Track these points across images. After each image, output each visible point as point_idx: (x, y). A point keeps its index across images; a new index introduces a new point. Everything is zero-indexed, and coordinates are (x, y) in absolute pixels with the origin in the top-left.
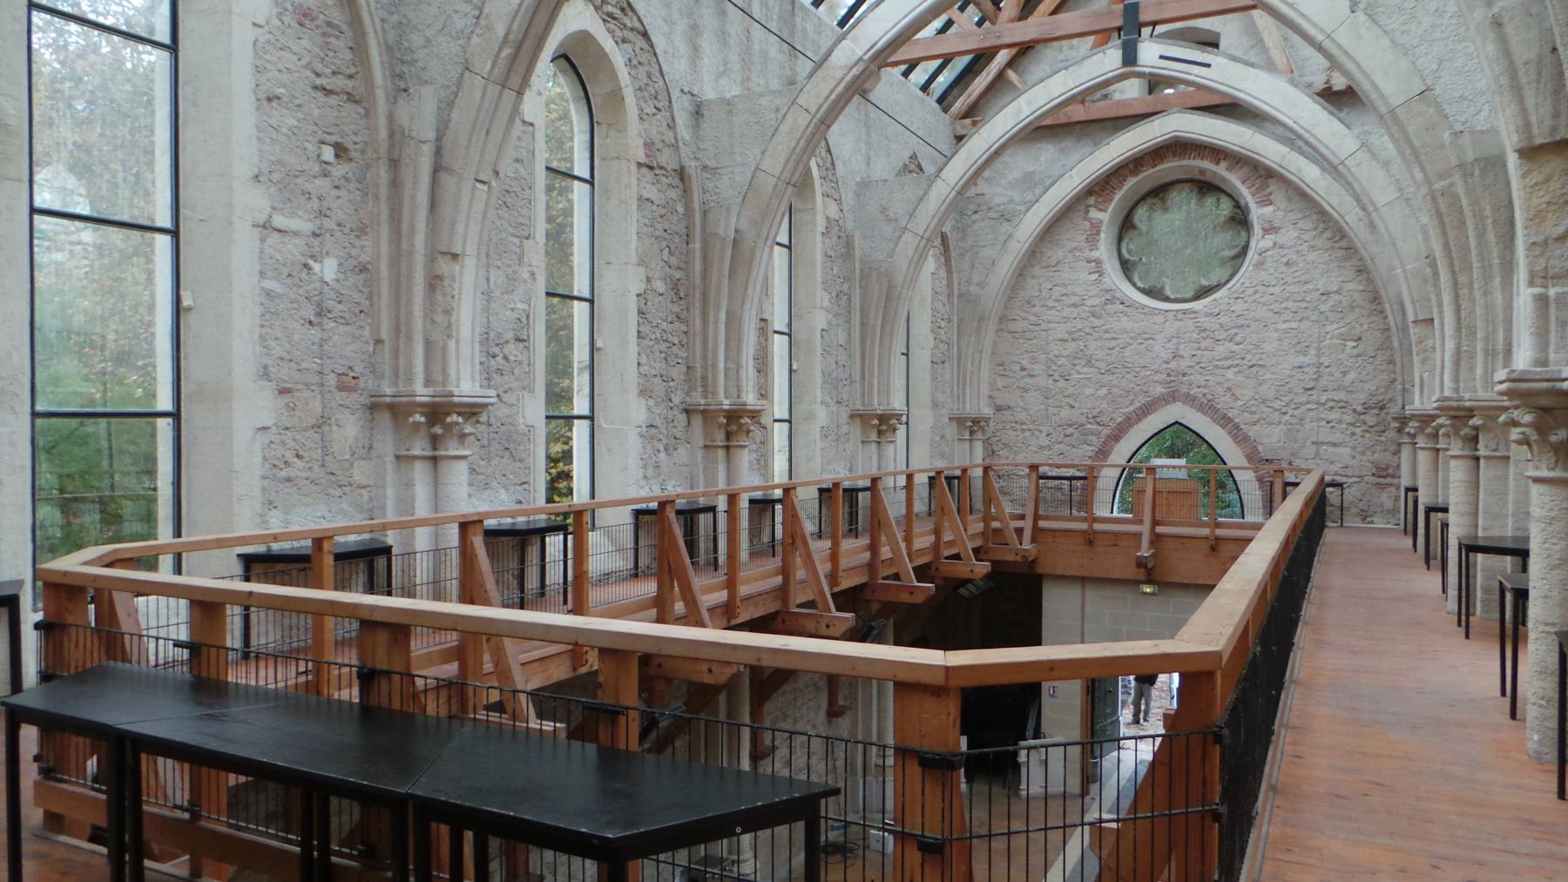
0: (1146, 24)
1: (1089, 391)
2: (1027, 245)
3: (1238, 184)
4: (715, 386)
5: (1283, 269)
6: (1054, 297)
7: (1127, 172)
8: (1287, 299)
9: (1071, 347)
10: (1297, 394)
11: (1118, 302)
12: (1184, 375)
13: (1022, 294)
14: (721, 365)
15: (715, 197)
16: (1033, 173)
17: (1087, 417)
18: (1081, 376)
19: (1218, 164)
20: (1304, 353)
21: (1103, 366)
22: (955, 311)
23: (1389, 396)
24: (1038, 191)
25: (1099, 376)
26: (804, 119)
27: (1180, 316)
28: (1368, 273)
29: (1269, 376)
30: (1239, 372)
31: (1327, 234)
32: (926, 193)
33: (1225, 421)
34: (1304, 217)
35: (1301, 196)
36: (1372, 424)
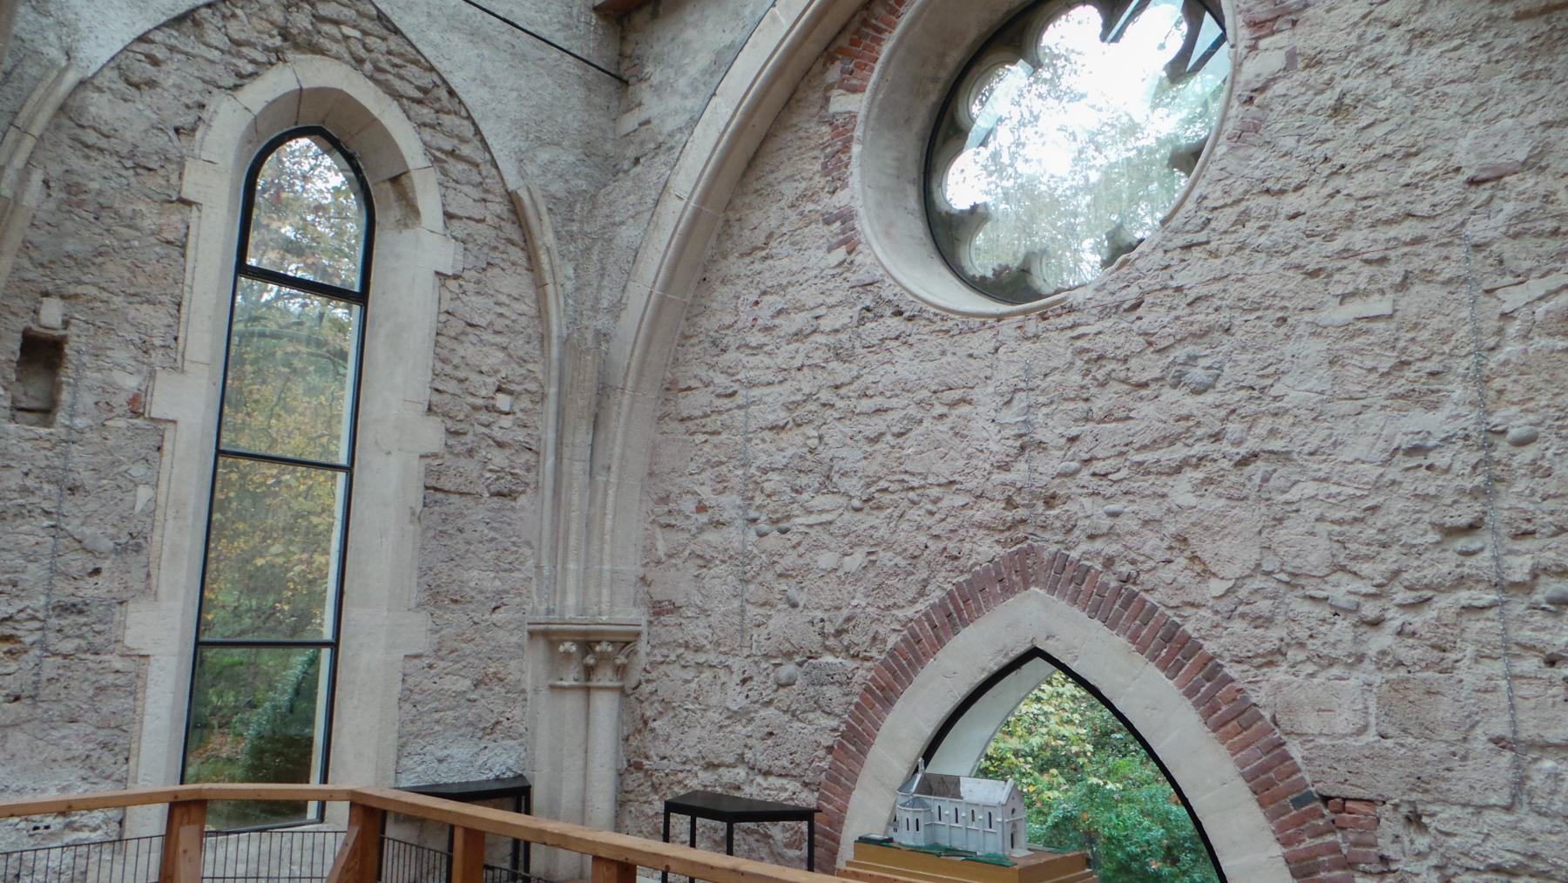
1: (826, 560)
5: (1327, 129)
8: (1349, 220)
9: (793, 442)
11: (888, 312)
13: (704, 322)
17: (822, 634)
21: (853, 485)
22: (554, 373)
25: (847, 516)
27: (1032, 327)
29: (1310, 488)
30: (1209, 481)
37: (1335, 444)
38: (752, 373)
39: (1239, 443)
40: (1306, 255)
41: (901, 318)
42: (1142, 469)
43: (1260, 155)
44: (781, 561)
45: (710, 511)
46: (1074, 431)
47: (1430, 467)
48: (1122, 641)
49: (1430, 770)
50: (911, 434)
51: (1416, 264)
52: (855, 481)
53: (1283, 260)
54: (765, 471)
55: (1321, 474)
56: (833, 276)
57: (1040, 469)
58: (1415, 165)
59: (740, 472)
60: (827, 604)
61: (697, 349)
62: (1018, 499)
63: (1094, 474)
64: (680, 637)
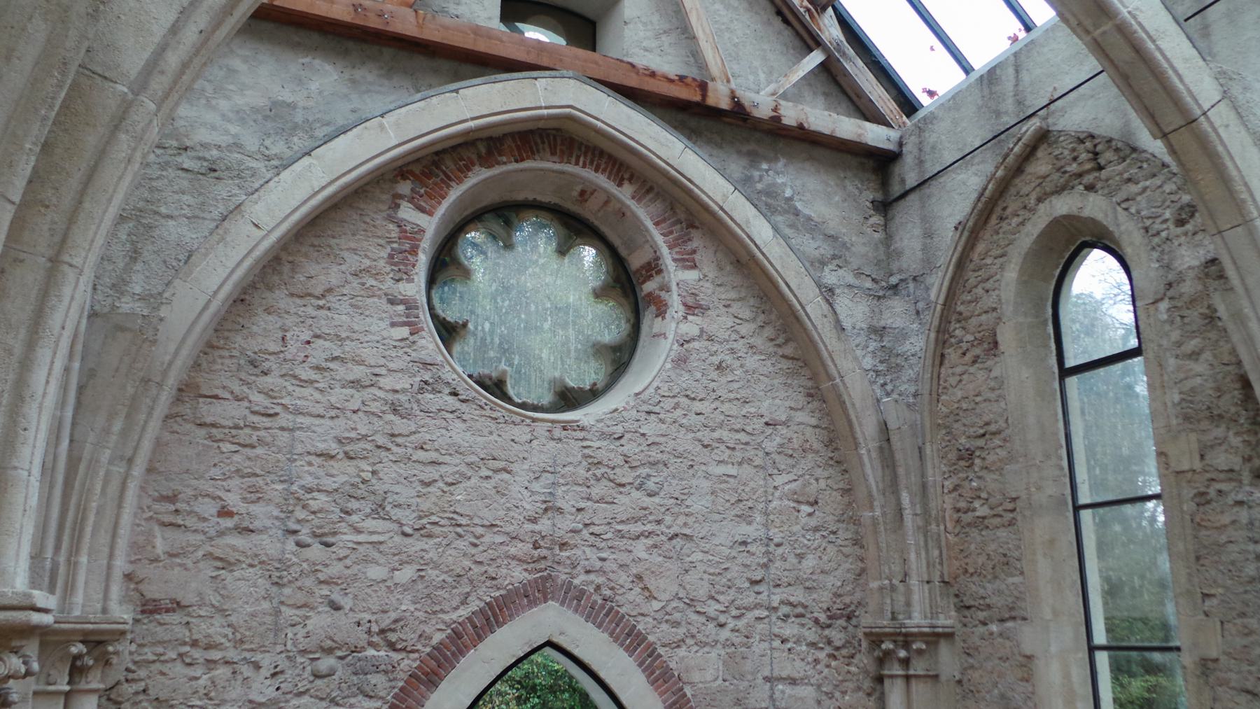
1: (375, 572)
3: (649, 224)
5: (714, 375)
7: (474, 157)
8: (721, 426)
9: (343, 473)
11: (447, 391)
12: (563, 545)
16: (292, 106)
17: (369, 632)
18: (361, 538)
19: (620, 185)
20: (745, 518)
21: (407, 517)
23: (858, 595)
24: (299, 142)
25: (398, 539)
27: (558, 433)
29: (699, 556)
30: (655, 546)
31: (769, 332)
33: (632, 640)
34: (740, 299)
36: (838, 644)
37: (712, 535)
38: (298, 402)
39: (669, 527)
40: (704, 436)
41: (456, 398)
42: (620, 535)
43: (686, 376)
44: (325, 570)
45: (236, 518)
46: (582, 505)
47: (748, 552)
48: (606, 635)
49: (742, 694)
50: (461, 485)
51: (747, 455)
52: (408, 512)
53: (693, 435)
54: (310, 491)
55: (706, 549)
56: (395, 347)
57: (559, 526)
58: (748, 409)
59: (279, 487)
60: (375, 608)
61: (227, 361)
62: (542, 543)
63: (592, 534)
64: (183, 633)
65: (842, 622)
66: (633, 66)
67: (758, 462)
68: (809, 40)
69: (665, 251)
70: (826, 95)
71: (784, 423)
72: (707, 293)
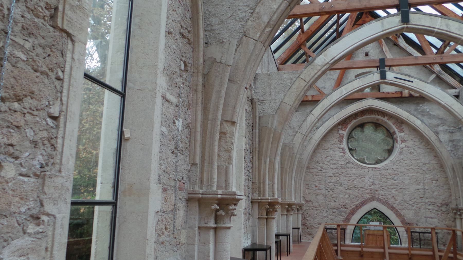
0: (387, 66)
1: (341, 196)
2: (318, 142)
3: (392, 125)
4: (264, 191)
5: (409, 155)
6: (327, 161)
8: (411, 165)
9: (334, 179)
10: (417, 199)
13: (315, 158)
14: (267, 182)
15: (262, 112)
17: (341, 206)
18: (338, 190)
19: (384, 117)
20: (419, 184)
21: (346, 186)
25: (345, 190)
26: (303, 84)
27: (374, 169)
28: (438, 157)
29: (407, 192)
30: (396, 190)
31: (423, 144)
32: (306, 119)
33: (392, 208)
34: (415, 137)
35: (414, 130)
36: (444, 211)
46: (380, 183)
48: (386, 207)
51: (418, 171)
58: (418, 161)
64: (312, 205)
65: (445, 206)
66: (384, 93)
67: (421, 172)
68: (433, 72)
69: (396, 130)
70: (438, 83)
71: (428, 164)
72: (406, 137)
